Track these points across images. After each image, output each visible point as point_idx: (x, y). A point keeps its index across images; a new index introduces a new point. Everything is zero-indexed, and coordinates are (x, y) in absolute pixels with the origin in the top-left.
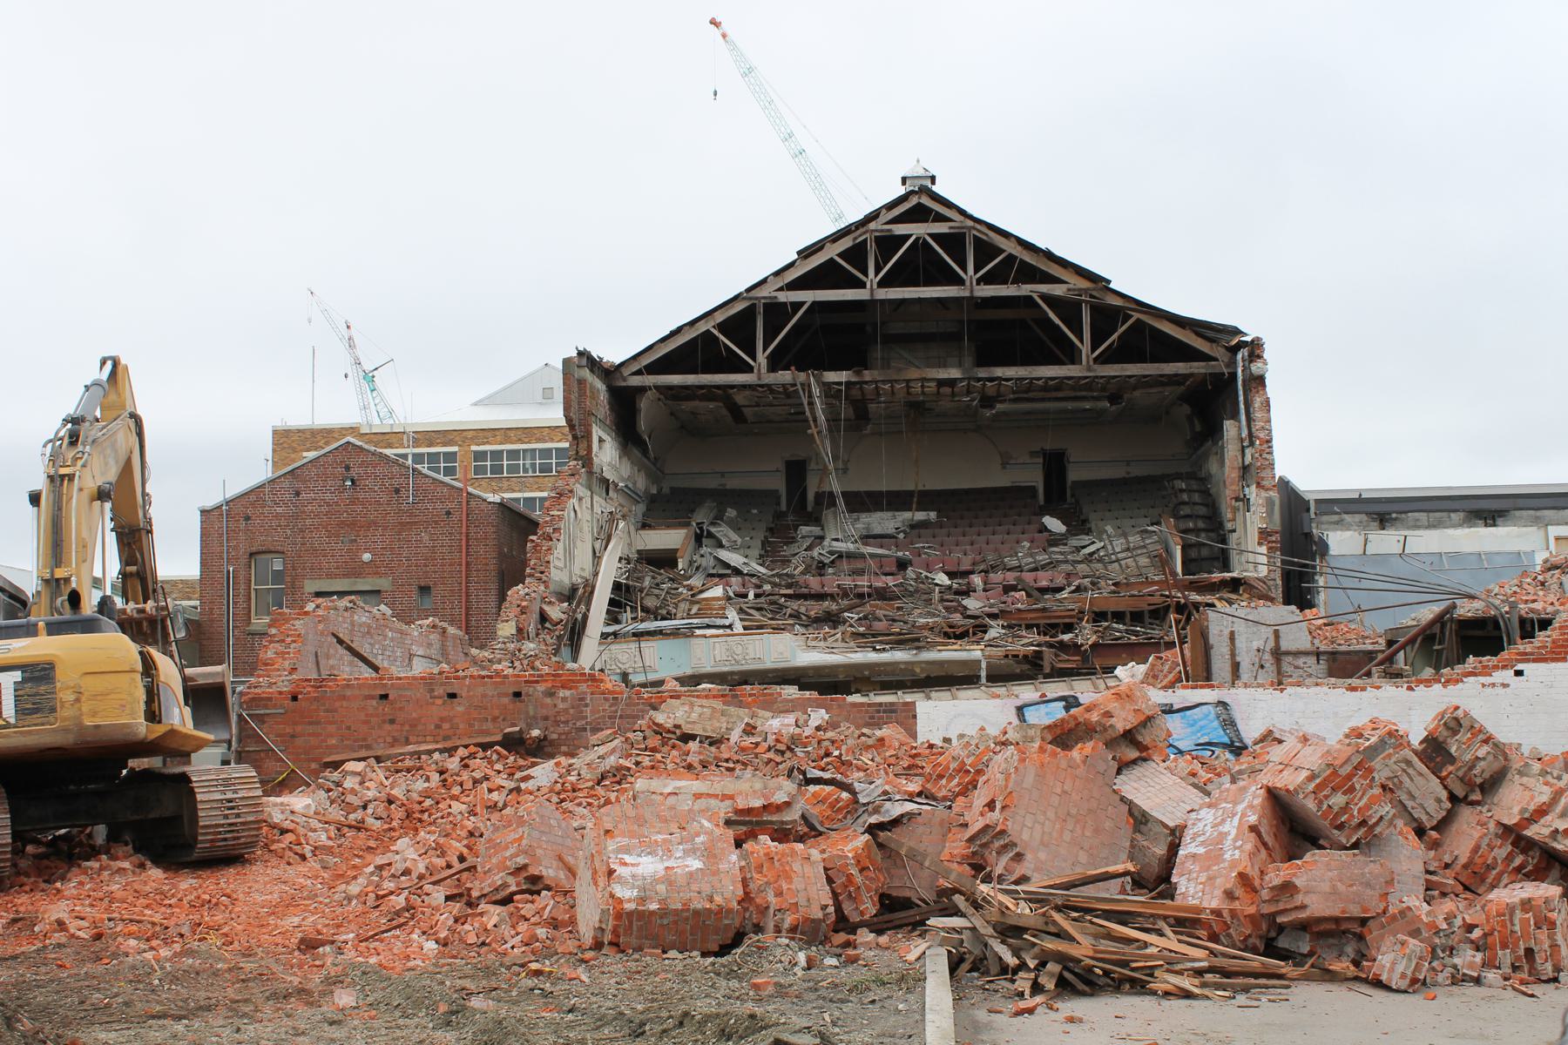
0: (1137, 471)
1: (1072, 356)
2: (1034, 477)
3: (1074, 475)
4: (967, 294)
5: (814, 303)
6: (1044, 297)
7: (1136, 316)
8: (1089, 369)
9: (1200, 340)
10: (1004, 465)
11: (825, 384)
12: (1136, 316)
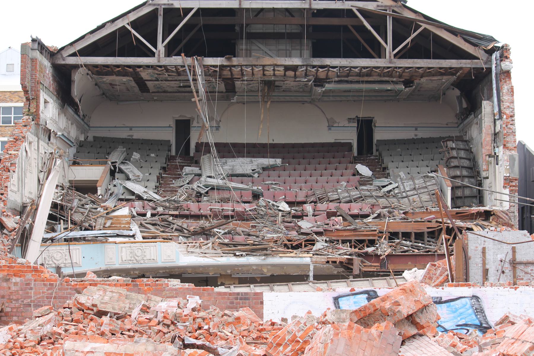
0: (422, 134)
1: (379, 52)
2: (350, 135)
3: (378, 135)
4: (307, 6)
5: (199, 9)
6: (360, 10)
7: (424, 26)
8: (390, 62)
9: (467, 44)
10: (330, 127)
11: (205, 66)
12: (424, 26)
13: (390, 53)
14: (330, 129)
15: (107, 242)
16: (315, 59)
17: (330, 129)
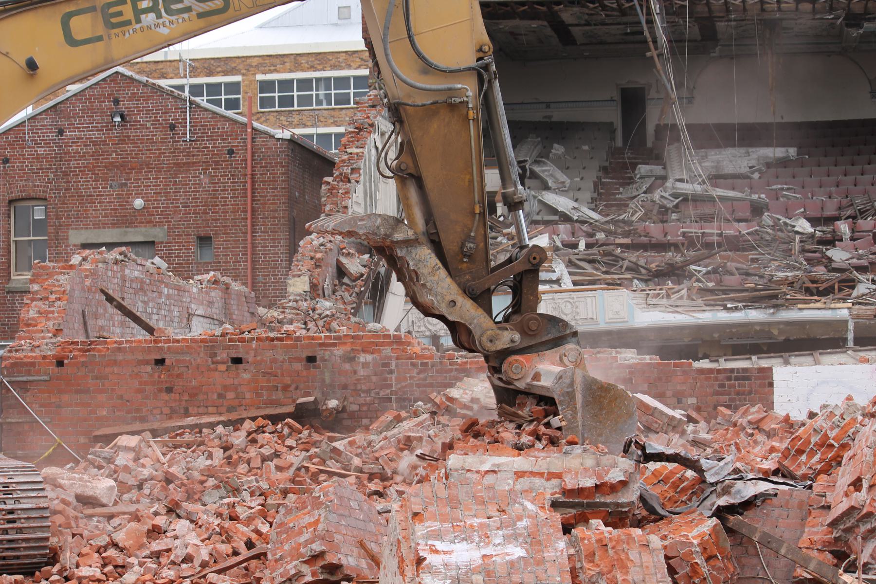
15: (216, 370)
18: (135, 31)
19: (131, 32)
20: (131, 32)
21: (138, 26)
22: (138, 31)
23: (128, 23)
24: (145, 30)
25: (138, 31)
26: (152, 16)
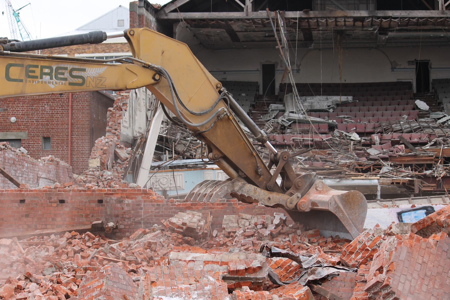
2: (410, 76)
3: (434, 75)
8: (443, 13)
10: (393, 69)
11: (286, 19)
13: (442, 5)
14: (393, 71)
16: (379, 11)
17: (393, 71)
18: (38, 82)
19: (37, 82)
20: (37, 82)
21: (40, 80)
22: (40, 82)
23: (36, 77)
24: (44, 82)
25: (40, 82)
26: (48, 77)
